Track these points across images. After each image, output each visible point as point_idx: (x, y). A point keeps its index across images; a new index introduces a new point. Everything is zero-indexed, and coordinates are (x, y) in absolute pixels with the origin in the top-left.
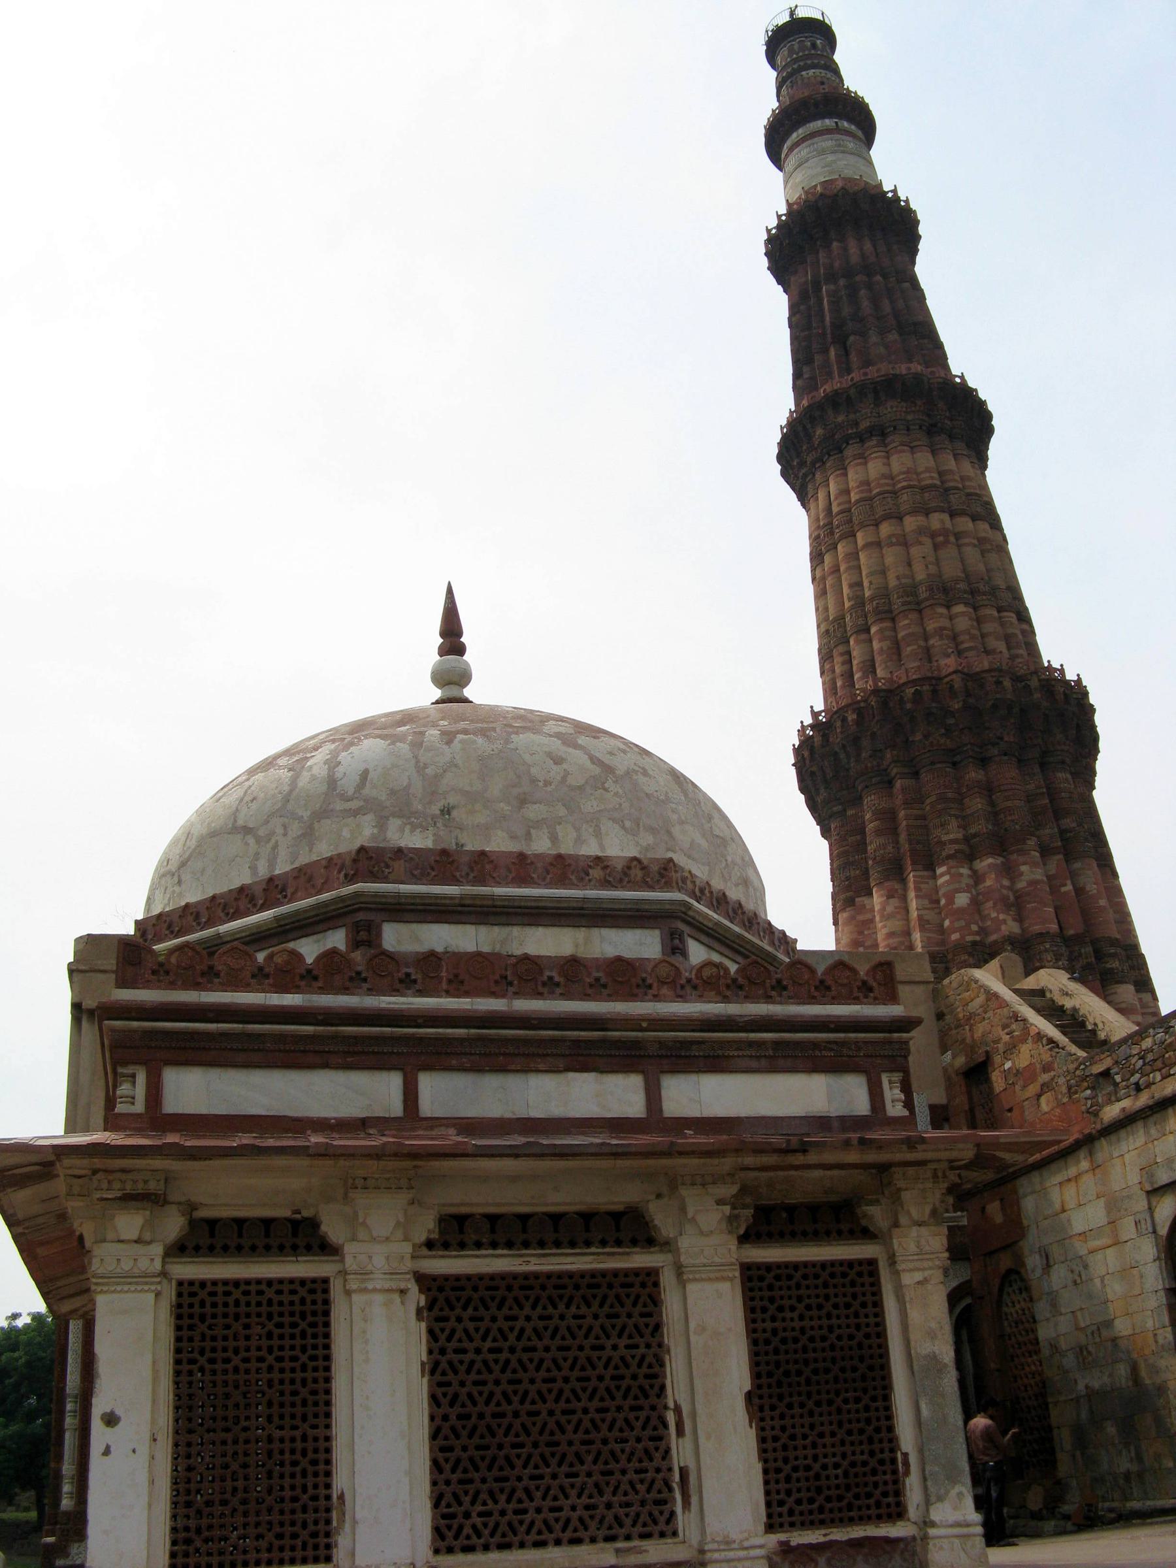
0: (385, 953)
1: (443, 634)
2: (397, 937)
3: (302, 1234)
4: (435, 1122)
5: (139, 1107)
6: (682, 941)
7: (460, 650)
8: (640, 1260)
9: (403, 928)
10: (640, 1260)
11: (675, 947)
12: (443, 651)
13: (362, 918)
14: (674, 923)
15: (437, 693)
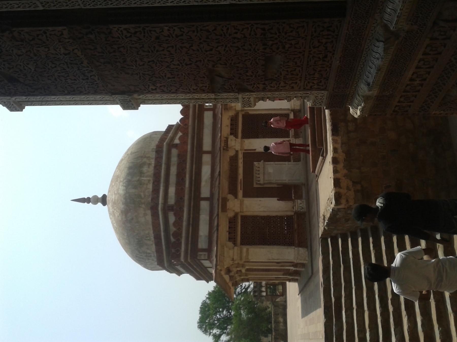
0: (175, 203)
1: (84, 202)
2: (172, 201)
3: (232, 222)
4: (212, 194)
5: (206, 253)
6: (175, 144)
7: (89, 198)
8: (241, 156)
9: (169, 200)
10: (241, 156)
11: (176, 146)
12: (88, 203)
13: (167, 208)
14: (171, 145)
15: (100, 204)
